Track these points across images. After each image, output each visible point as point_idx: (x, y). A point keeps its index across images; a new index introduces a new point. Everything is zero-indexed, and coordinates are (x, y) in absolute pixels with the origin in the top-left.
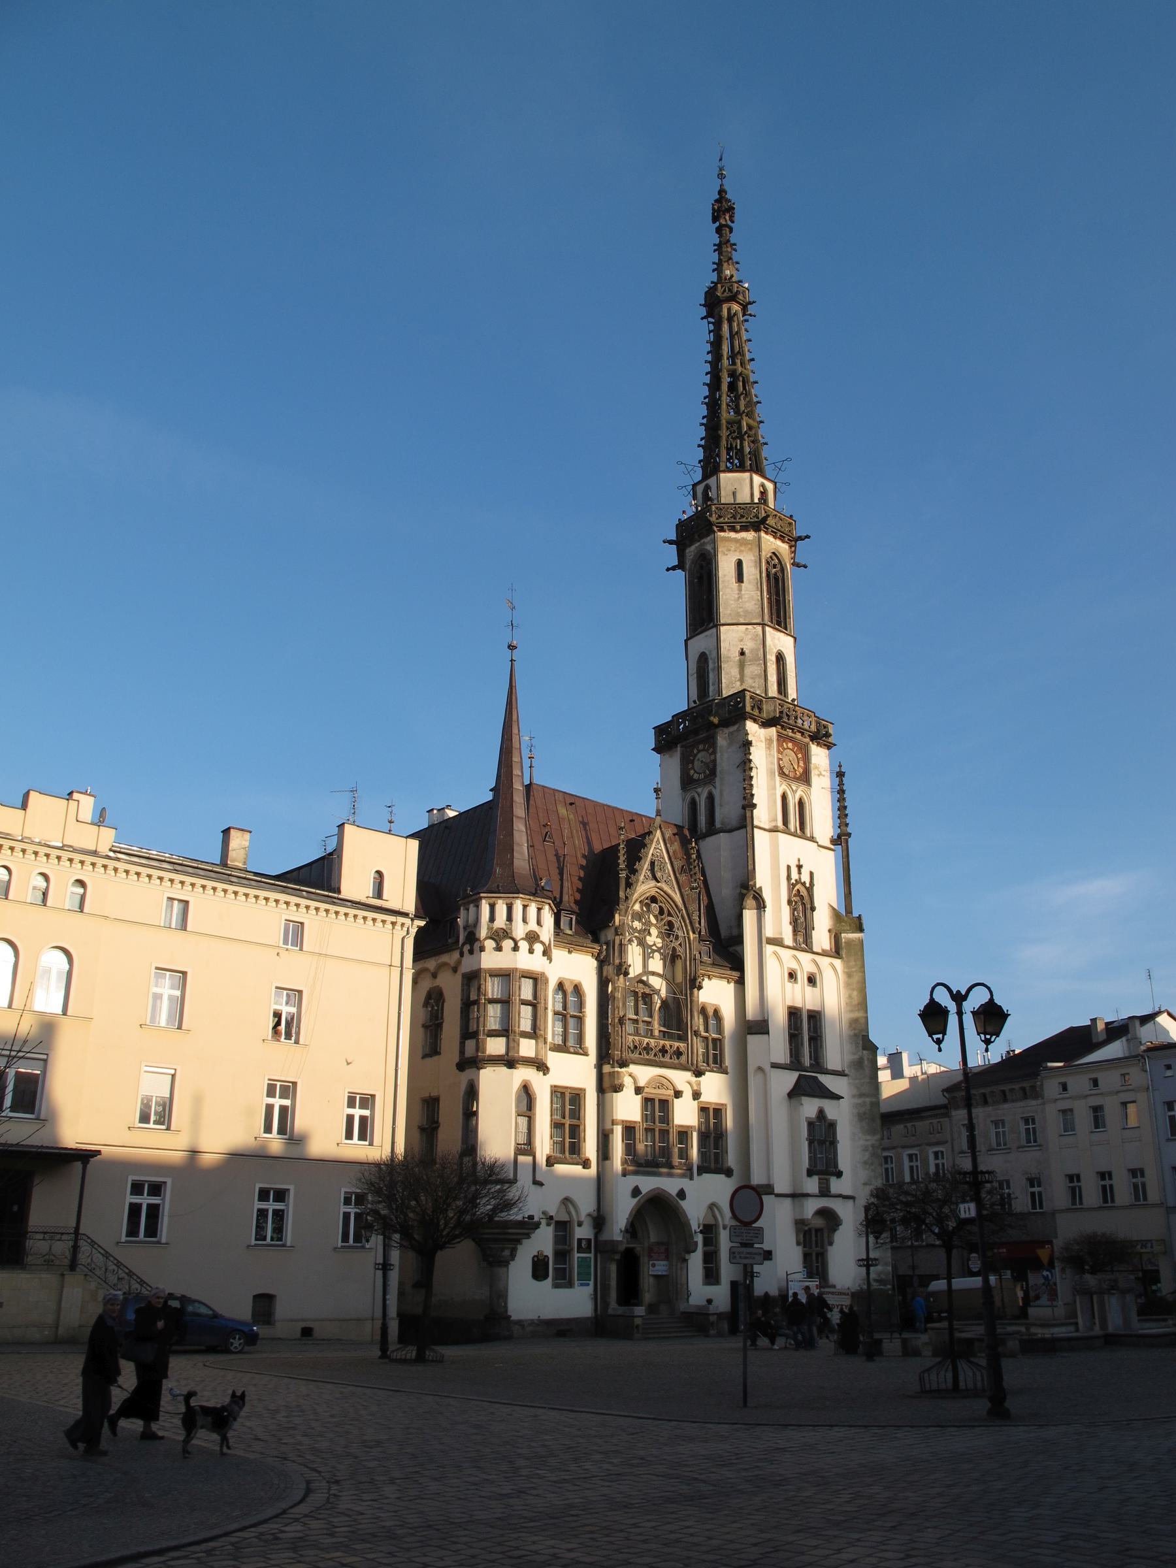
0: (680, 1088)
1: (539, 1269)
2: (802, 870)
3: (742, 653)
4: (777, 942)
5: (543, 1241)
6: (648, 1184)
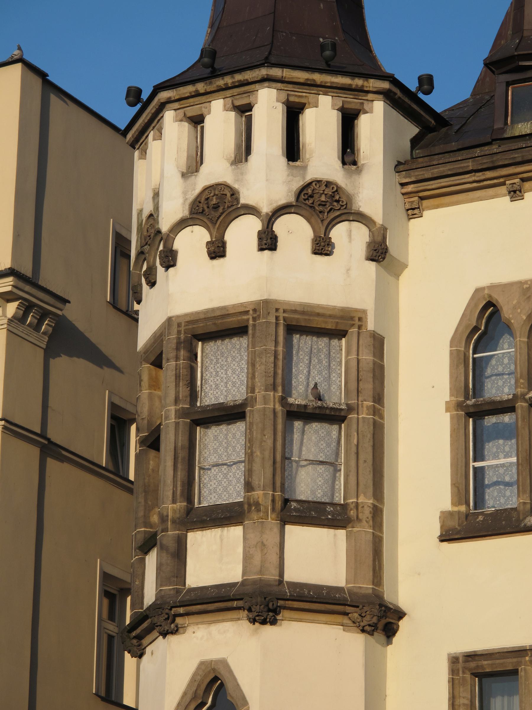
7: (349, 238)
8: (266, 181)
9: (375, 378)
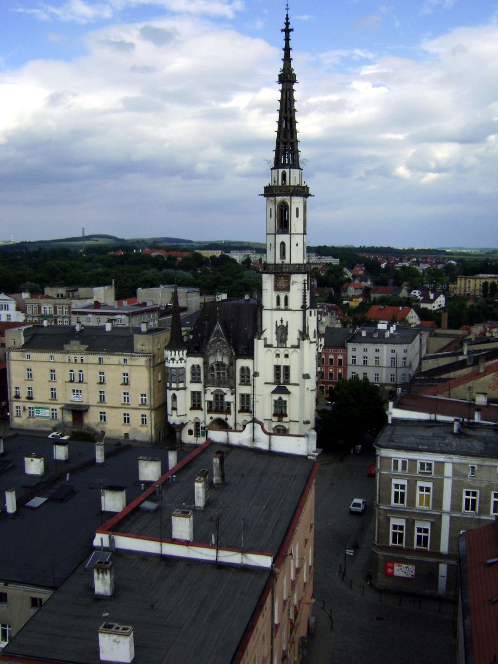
0: (225, 392)
1: (190, 432)
2: (283, 322)
3: (271, 245)
4: (271, 346)
5: (192, 427)
6: (215, 416)
7: (183, 361)
8: (177, 358)
9: (184, 372)
